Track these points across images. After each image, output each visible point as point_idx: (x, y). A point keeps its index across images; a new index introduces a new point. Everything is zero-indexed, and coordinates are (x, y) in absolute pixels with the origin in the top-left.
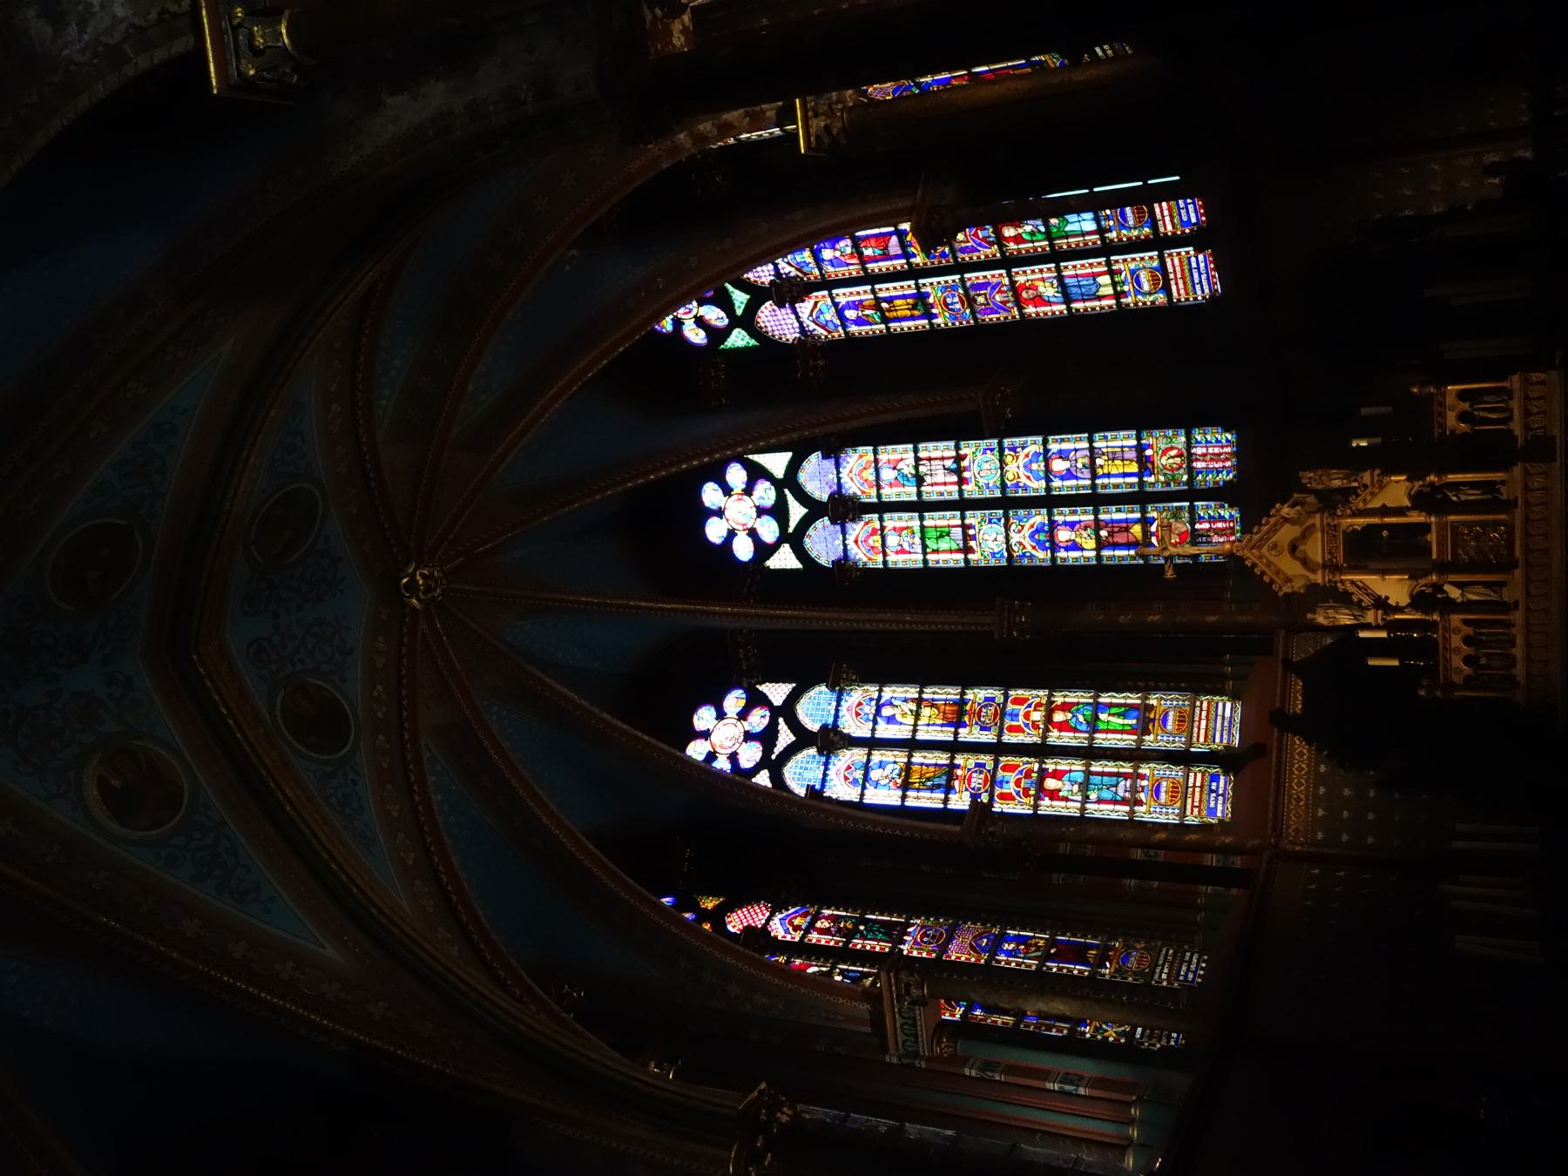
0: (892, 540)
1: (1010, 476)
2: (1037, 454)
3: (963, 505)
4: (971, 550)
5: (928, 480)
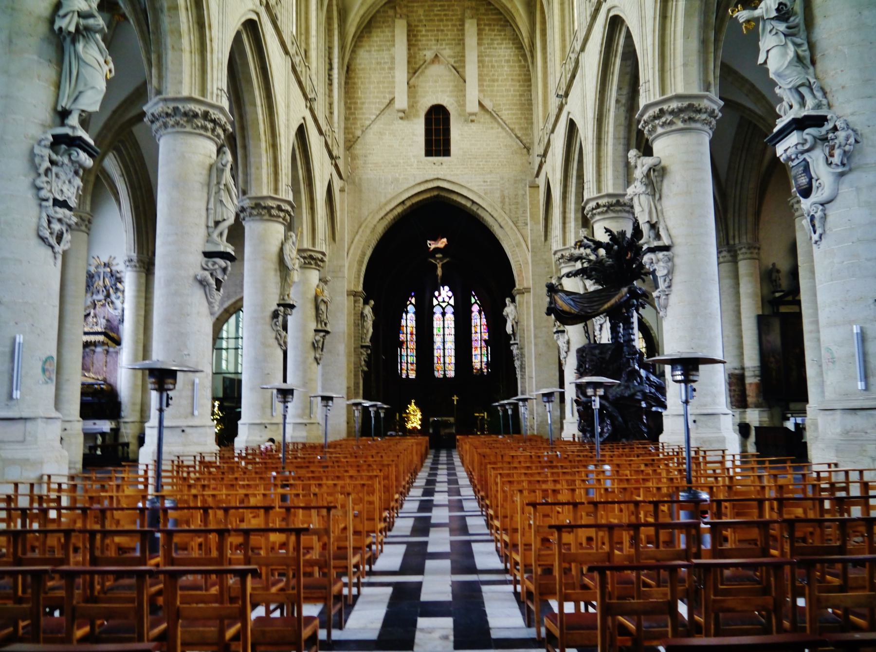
3: (444, 335)
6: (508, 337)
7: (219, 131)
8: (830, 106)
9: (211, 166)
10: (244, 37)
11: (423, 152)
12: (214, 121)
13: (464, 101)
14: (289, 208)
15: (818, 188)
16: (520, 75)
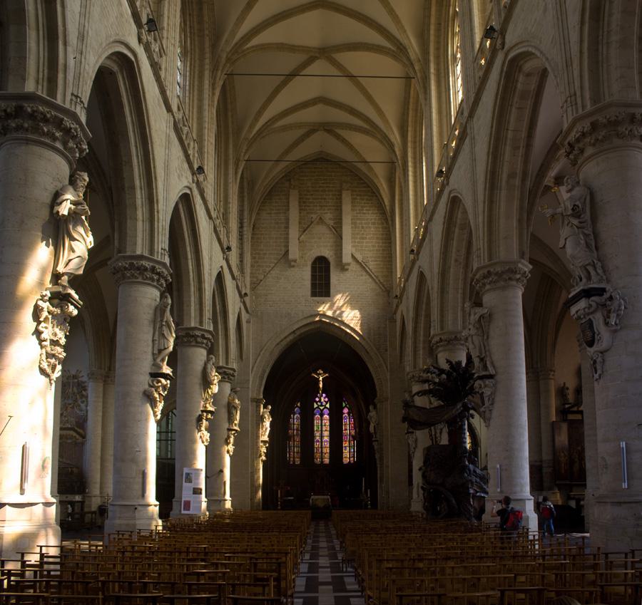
3: (322, 431)
6: (370, 435)
7: (163, 282)
8: (608, 281)
9: (156, 308)
10: (180, 206)
11: (309, 293)
12: (158, 274)
13: (341, 253)
14: (211, 337)
15: (598, 340)
16: (383, 234)
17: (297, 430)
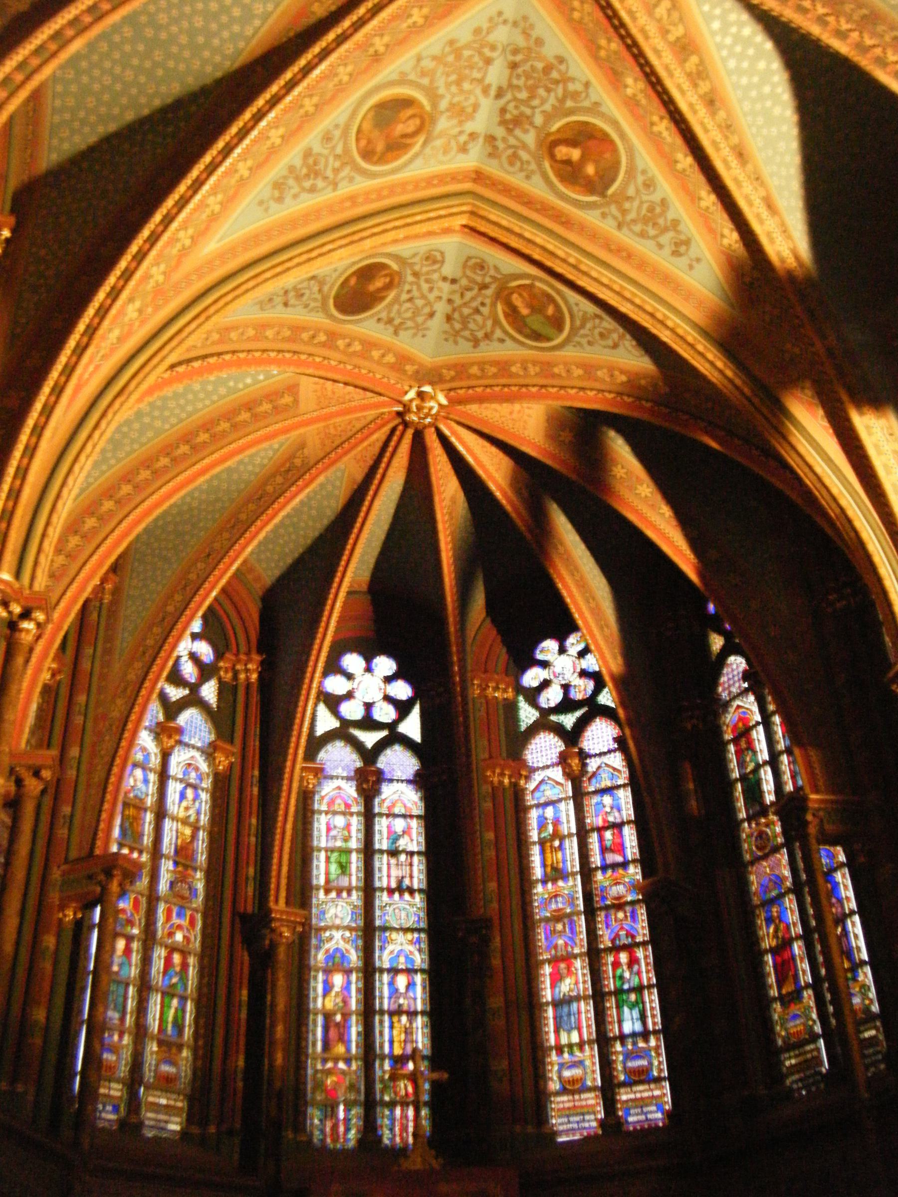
0: (340, 821)
1: (394, 935)
2: (413, 961)
3: (369, 890)
4: (327, 891)
5: (393, 861)
17: (183, 854)
